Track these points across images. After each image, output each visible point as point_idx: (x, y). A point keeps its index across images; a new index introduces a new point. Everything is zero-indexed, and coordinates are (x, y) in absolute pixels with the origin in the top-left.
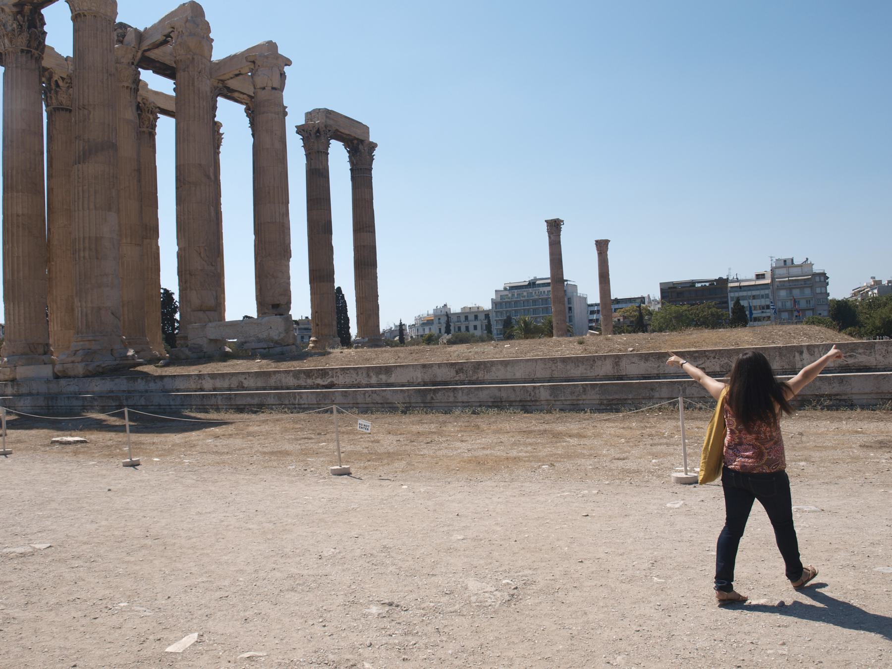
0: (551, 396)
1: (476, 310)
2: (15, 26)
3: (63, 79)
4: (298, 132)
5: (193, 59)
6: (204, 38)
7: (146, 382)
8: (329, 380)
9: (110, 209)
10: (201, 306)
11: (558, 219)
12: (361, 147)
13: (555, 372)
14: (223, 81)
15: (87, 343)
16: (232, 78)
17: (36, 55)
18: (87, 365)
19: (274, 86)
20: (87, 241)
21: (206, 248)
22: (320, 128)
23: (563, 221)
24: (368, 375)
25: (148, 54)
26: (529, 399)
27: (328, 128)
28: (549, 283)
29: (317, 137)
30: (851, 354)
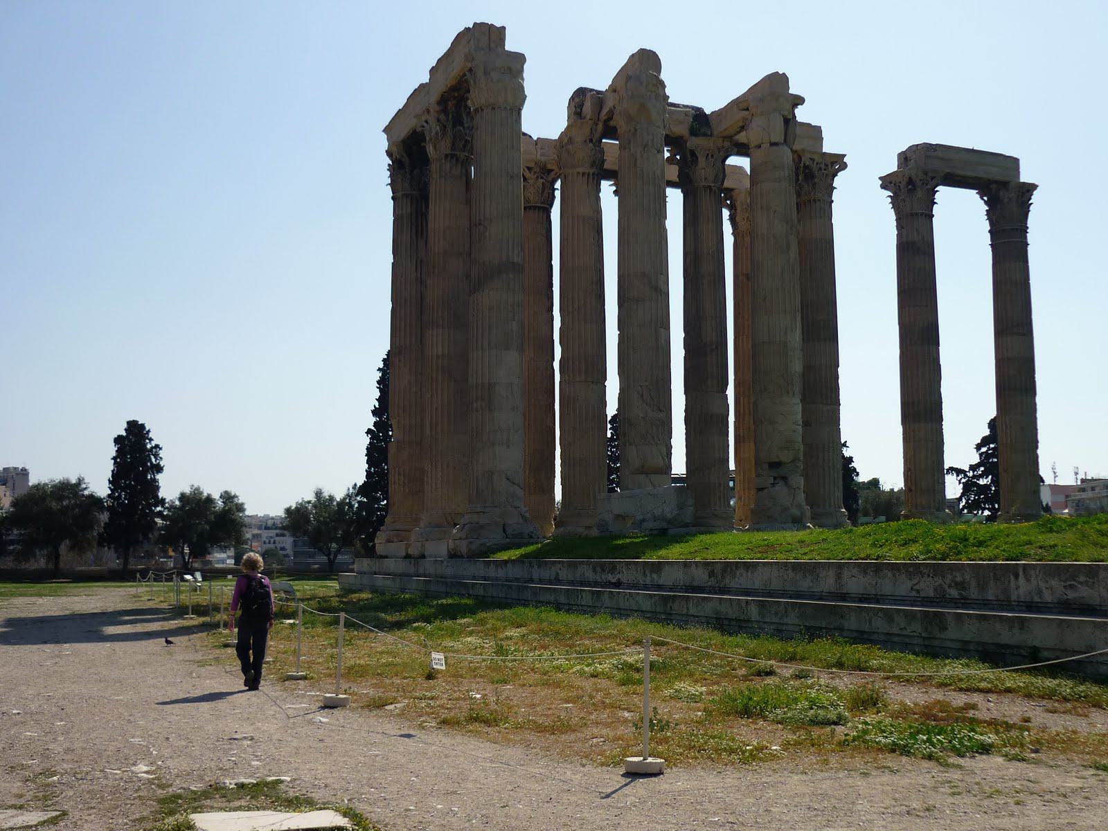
2: (438, 128)
3: (529, 169)
4: (883, 187)
10: (643, 466)
14: (730, 138)
15: (475, 515)
19: (773, 141)
22: (914, 178)
24: (645, 575)
26: (742, 618)
27: (930, 174)
29: (909, 191)
30: (1072, 583)
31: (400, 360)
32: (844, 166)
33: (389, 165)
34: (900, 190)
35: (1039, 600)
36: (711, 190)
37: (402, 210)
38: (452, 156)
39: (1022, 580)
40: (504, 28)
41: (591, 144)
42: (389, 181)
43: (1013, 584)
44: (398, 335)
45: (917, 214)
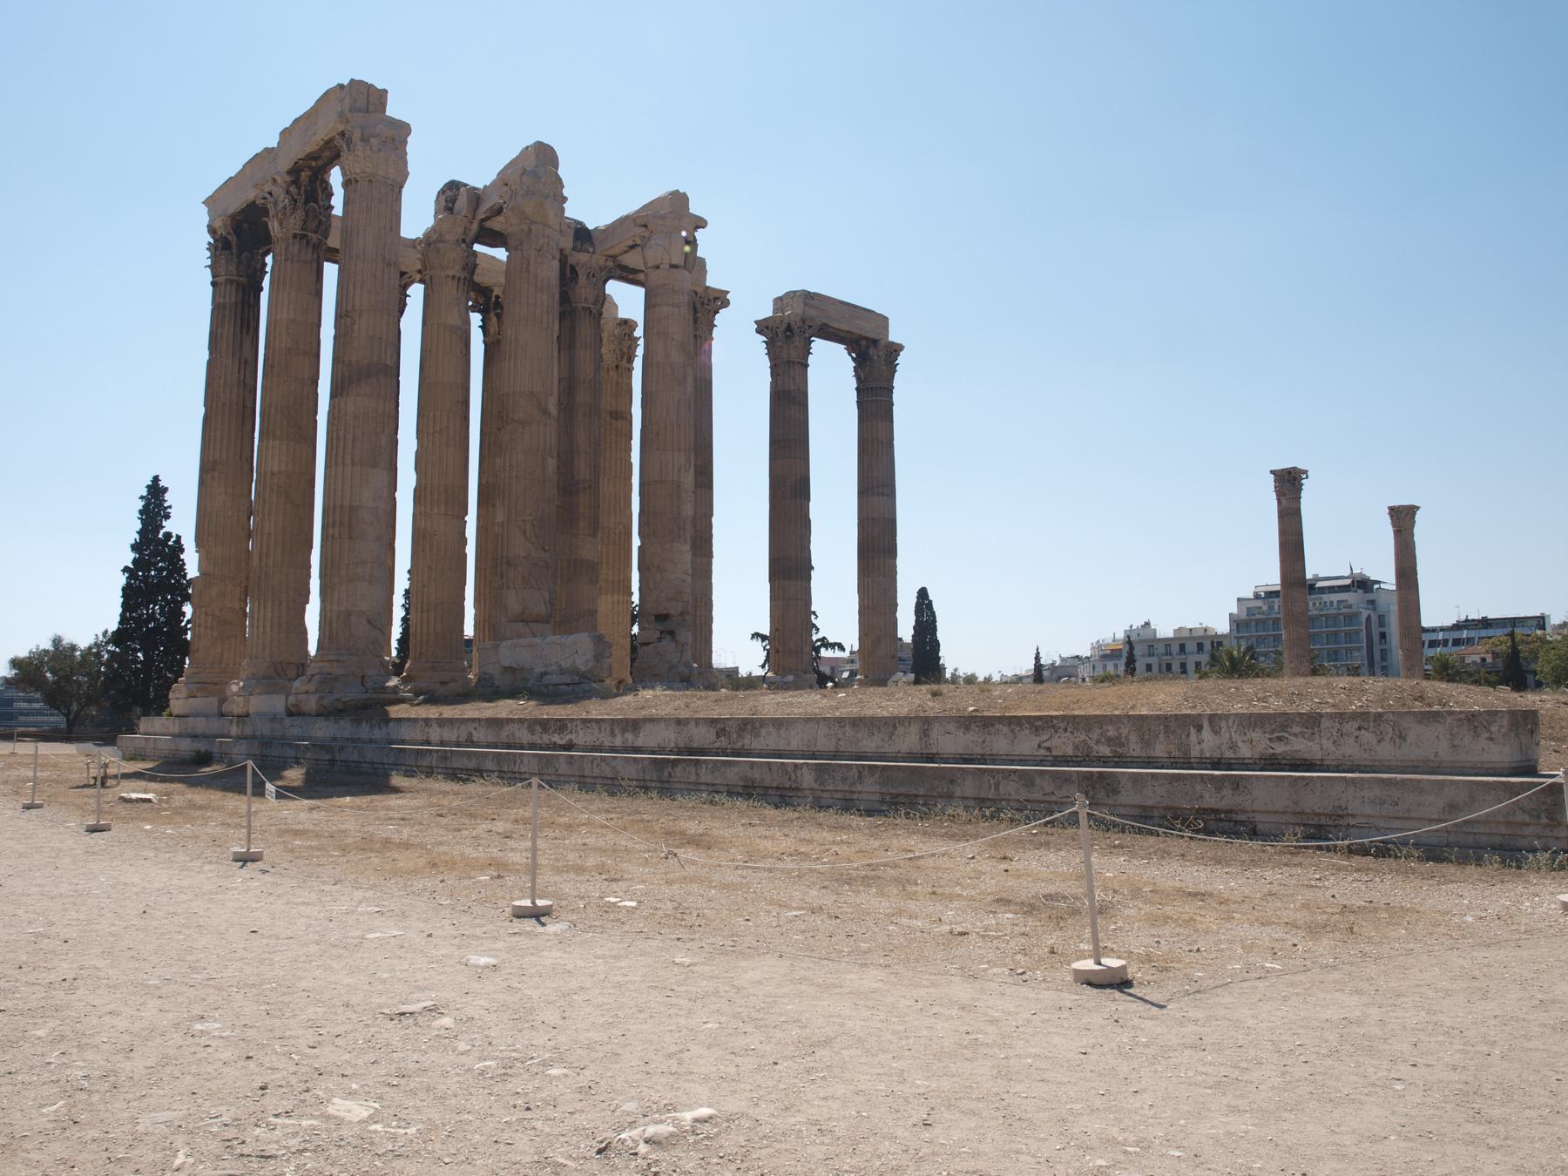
0: (816, 782)
1: (1202, 633)
2: (287, 201)
4: (759, 331)
5: (530, 230)
6: (548, 196)
7: (371, 727)
8: (568, 738)
9: (374, 465)
10: (523, 613)
11: (1295, 468)
12: (872, 351)
13: (841, 743)
14: (614, 257)
15: (327, 664)
16: (625, 252)
17: (315, 240)
18: (322, 698)
19: (673, 262)
20: (338, 512)
21: (535, 523)
22: (793, 324)
23: (1306, 472)
24: (613, 734)
25: (488, 224)
26: (788, 786)
27: (808, 323)
28: (1278, 592)
29: (787, 337)
30: (1281, 734)
31: (213, 478)
32: (726, 304)
33: (209, 243)
34: (777, 335)
35: (1233, 756)
36: (591, 312)
37: (224, 297)
38: (303, 237)
39: (1207, 733)
41: (464, 245)
42: (209, 262)
43: (1193, 738)
44: (212, 447)
45: (794, 362)
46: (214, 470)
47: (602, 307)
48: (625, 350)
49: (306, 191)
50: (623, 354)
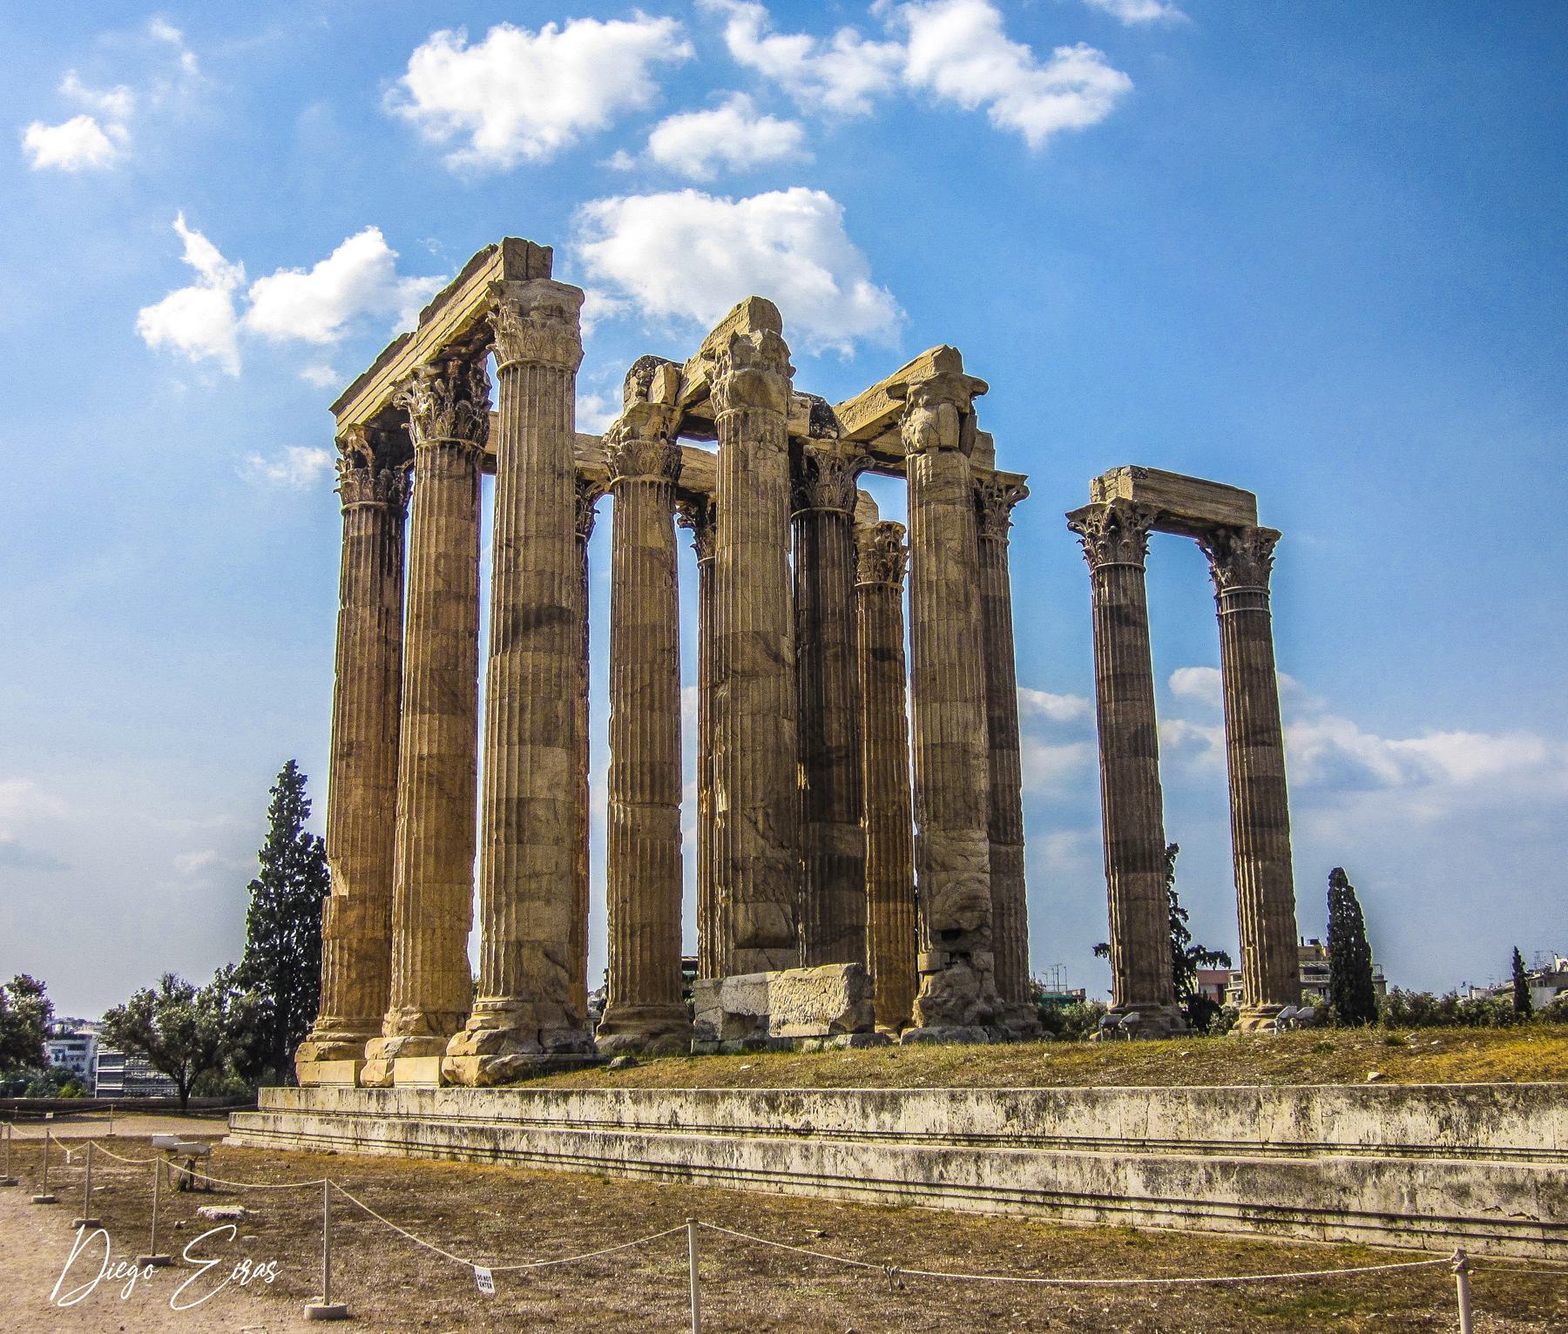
0: (1146, 1187)
7: (545, 1102)
8: (804, 1119)
9: (549, 742)
12: (1234, 543)
16: (881, 434)
17: (469, 448)
18: (484, 1063)
19: (945, 442)
20: (503, 807)
21: (770, 811)
24: (865, 1116)
25: (694, 411)
26: (1106, 1193)
31: (348, 766)
32: (1023, 494)
36: (838, 518)
40: (550, 250)
41: (663, 441)
45: (1123, 567)
46: (349, 755)
47: (853, 510)
48: (890, 564)
49: (455, 386)
50: (887, 571)
